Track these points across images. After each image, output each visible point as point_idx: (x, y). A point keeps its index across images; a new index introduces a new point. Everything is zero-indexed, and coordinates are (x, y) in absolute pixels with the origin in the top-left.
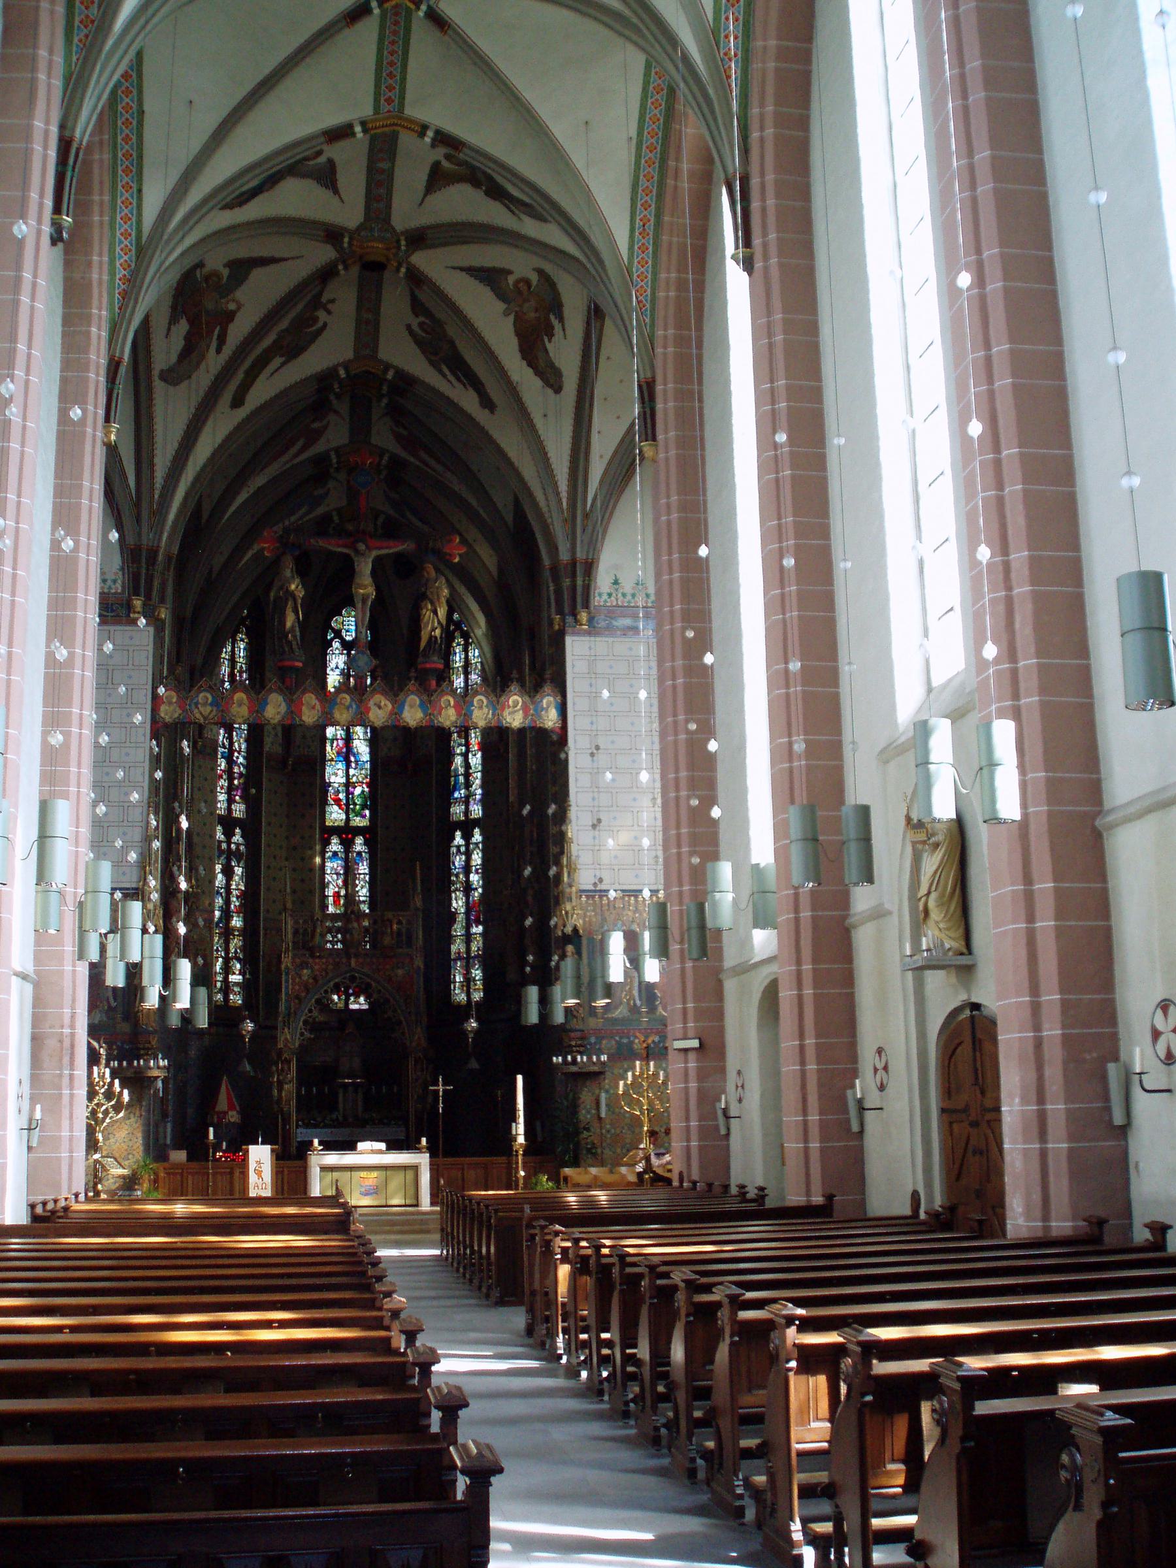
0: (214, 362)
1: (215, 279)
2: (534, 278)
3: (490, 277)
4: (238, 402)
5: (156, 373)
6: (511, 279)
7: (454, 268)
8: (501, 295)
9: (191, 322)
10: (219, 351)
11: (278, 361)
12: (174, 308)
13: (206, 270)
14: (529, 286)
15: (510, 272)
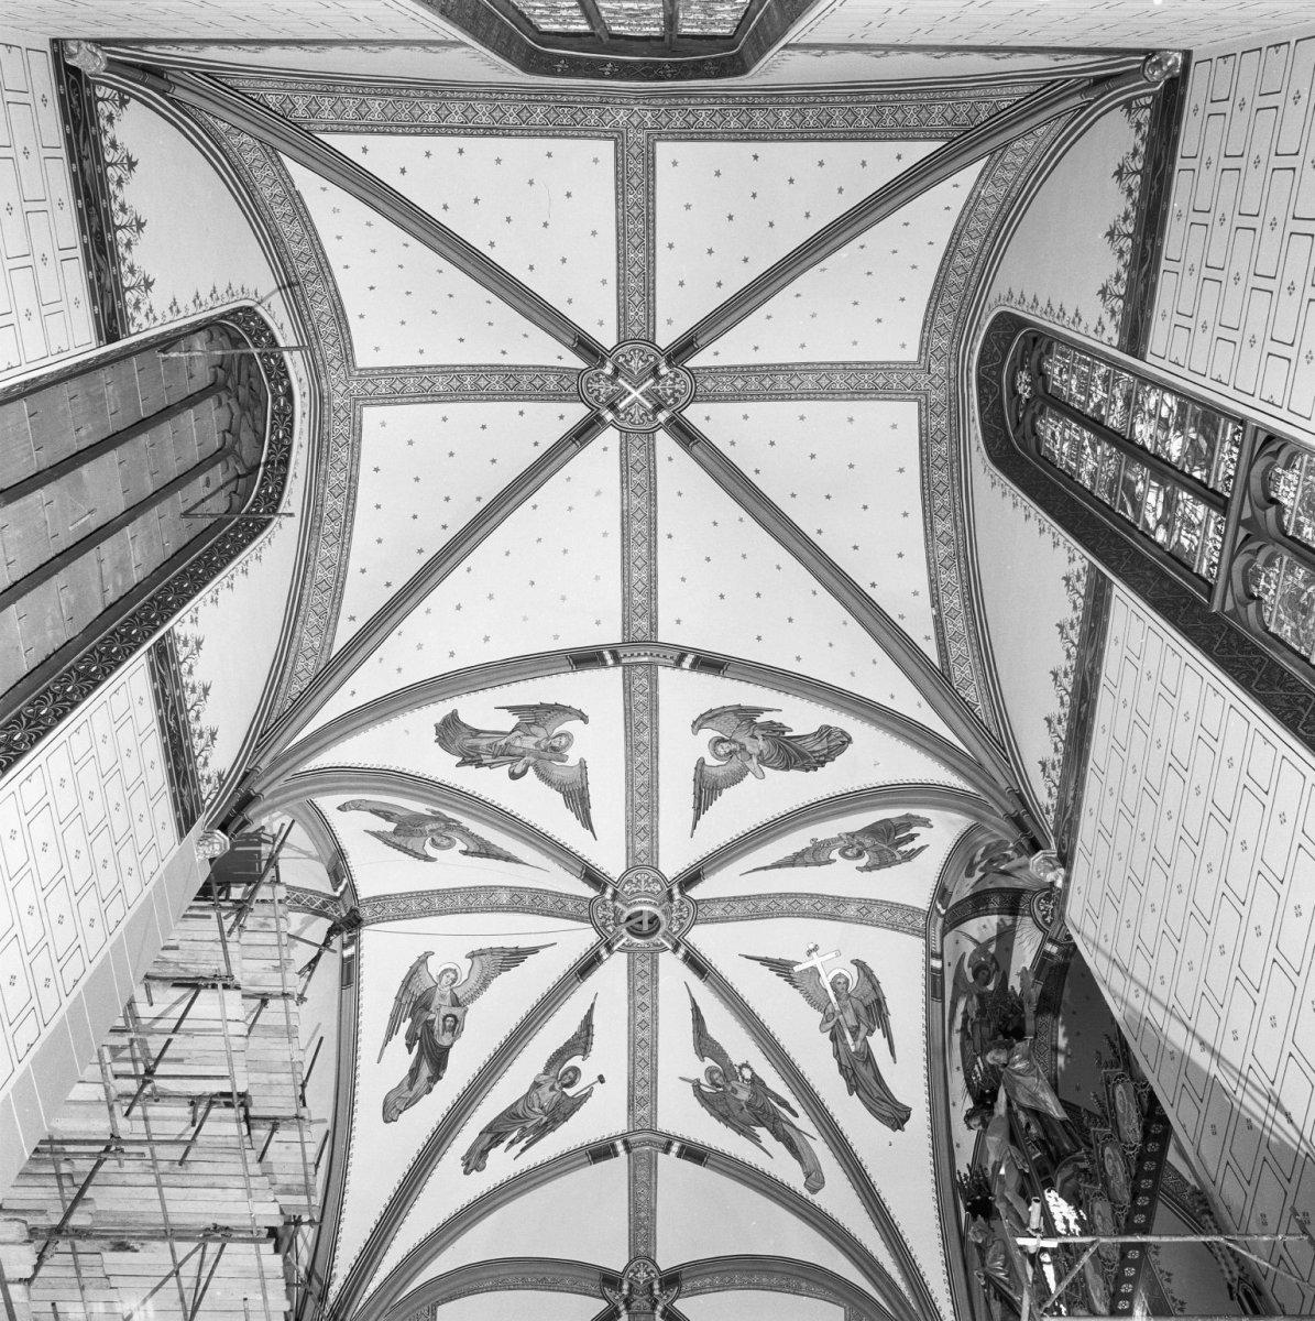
0: (804, 1122)
1: (716, 1076)
2: (708, 734)
3: (706, 791)
4: (897, 1117)
5: (805, 1193)
6: (711, 761)
7: (694, 827)
8: (736, 778)
9: (762, 1125)
10: (796, 1116)
11: (877, 1042)
12: (741, 1132)
13: (704, 1081)
14: (723, 740)
15: (701, 762)
